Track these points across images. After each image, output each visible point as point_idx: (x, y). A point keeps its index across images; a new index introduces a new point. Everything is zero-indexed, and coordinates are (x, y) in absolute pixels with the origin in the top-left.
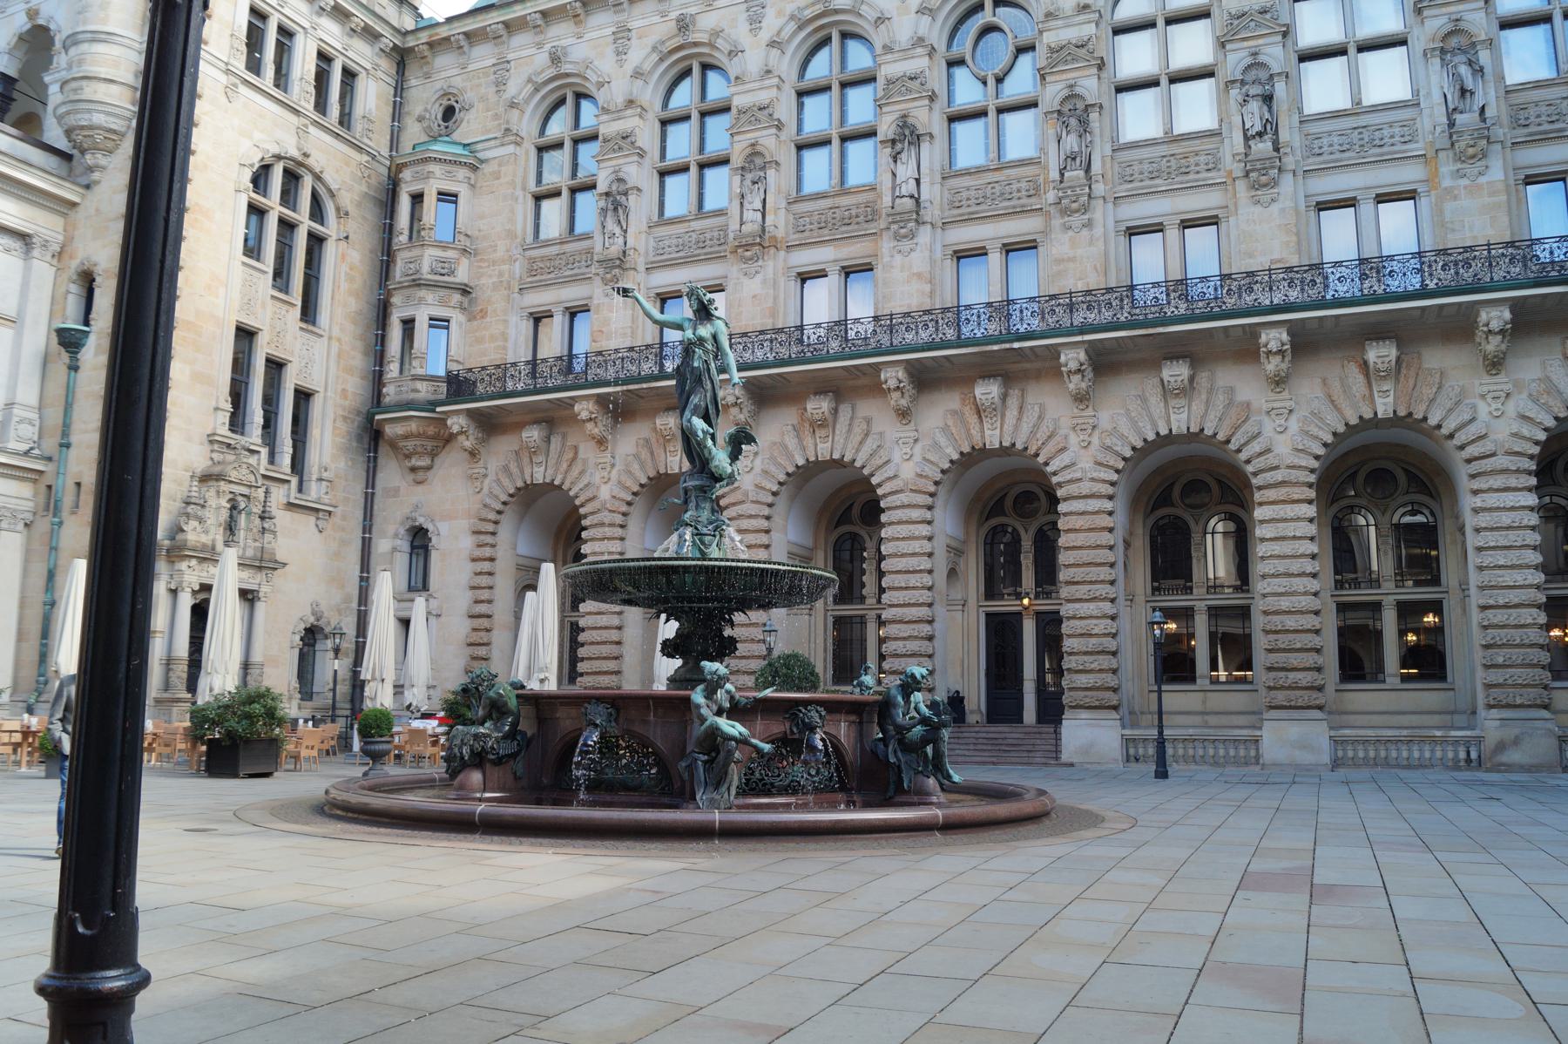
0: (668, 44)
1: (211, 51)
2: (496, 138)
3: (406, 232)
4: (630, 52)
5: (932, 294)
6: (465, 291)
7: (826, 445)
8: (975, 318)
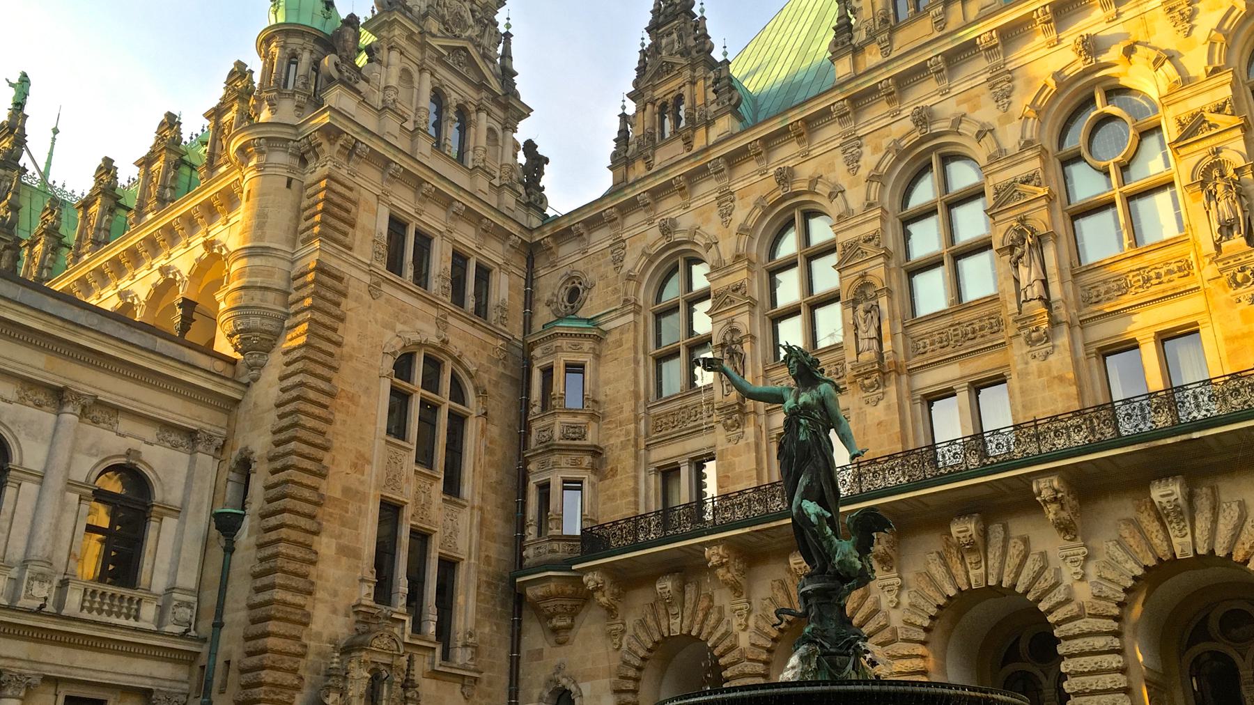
0: (768, 199)
1: (355, 255)
2: (616, 310)
3: (539, 404)
4: (734, 212)
5: (1081, 394)
6: (596, 452)
7: (978, 571)
8: (1138, 411)
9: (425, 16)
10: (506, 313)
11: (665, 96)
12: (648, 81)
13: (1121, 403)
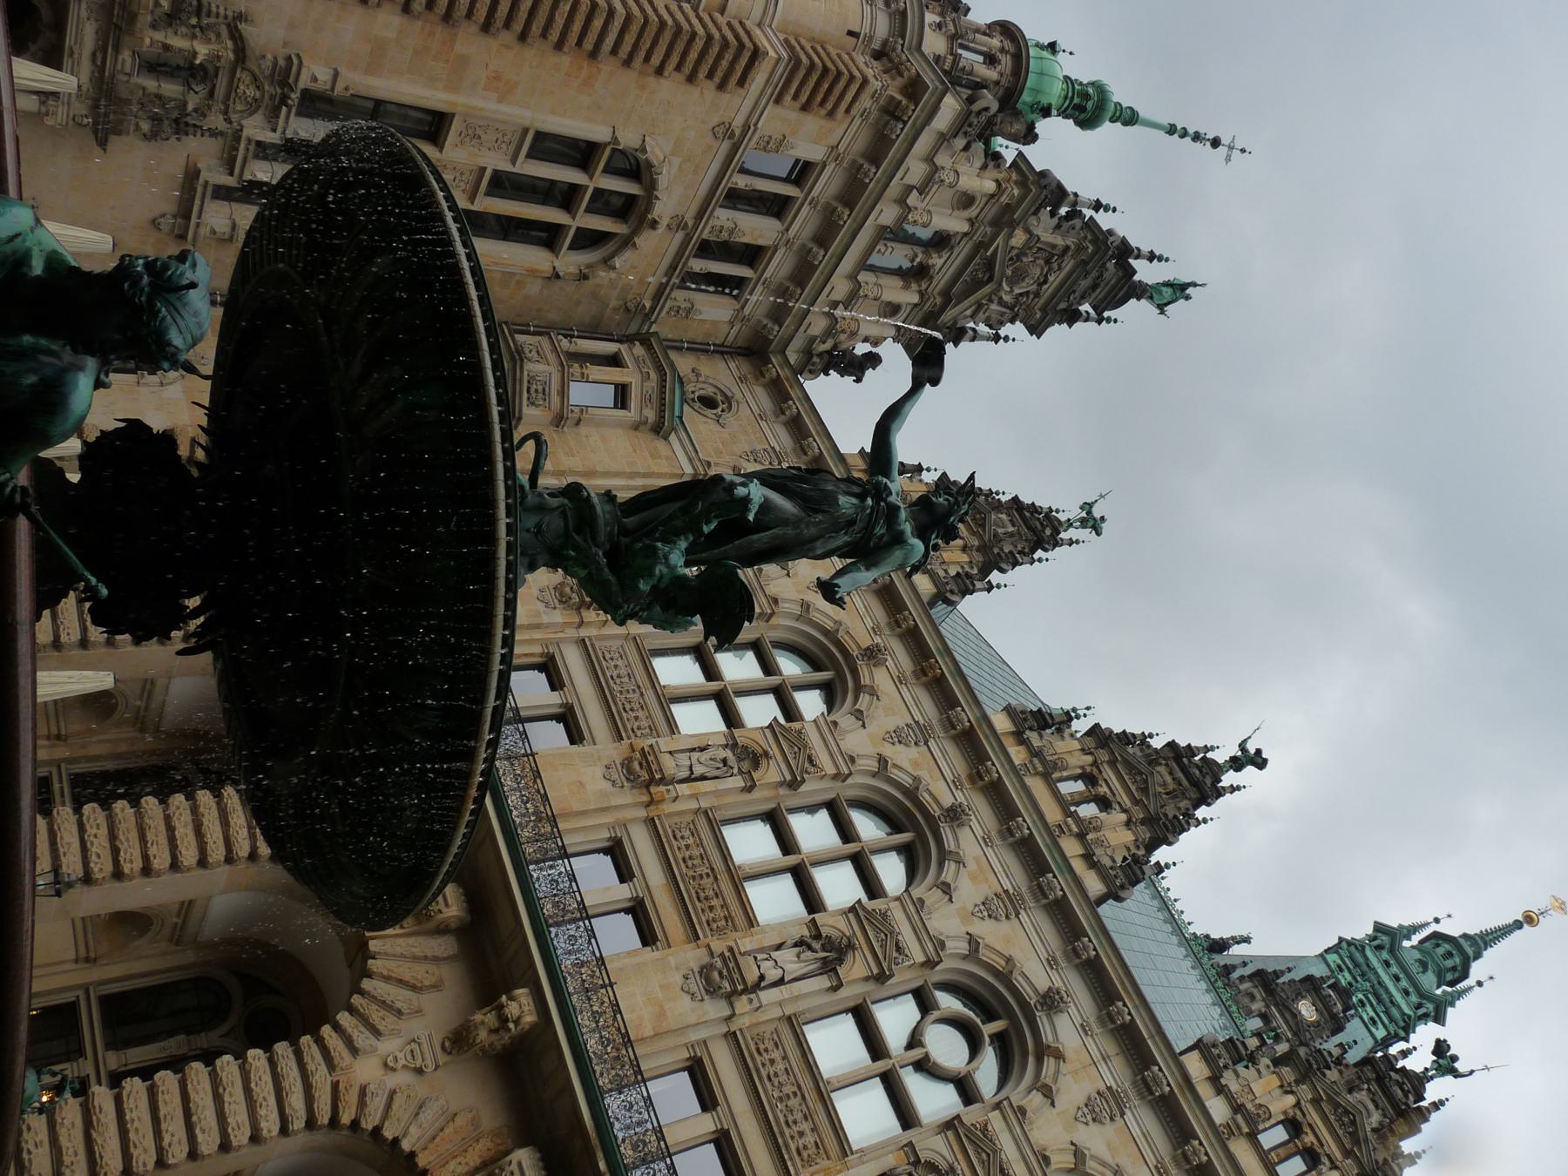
1: (769, 107)
3: (573, 348)
9: (1028, 231)
13: (645, 1094)
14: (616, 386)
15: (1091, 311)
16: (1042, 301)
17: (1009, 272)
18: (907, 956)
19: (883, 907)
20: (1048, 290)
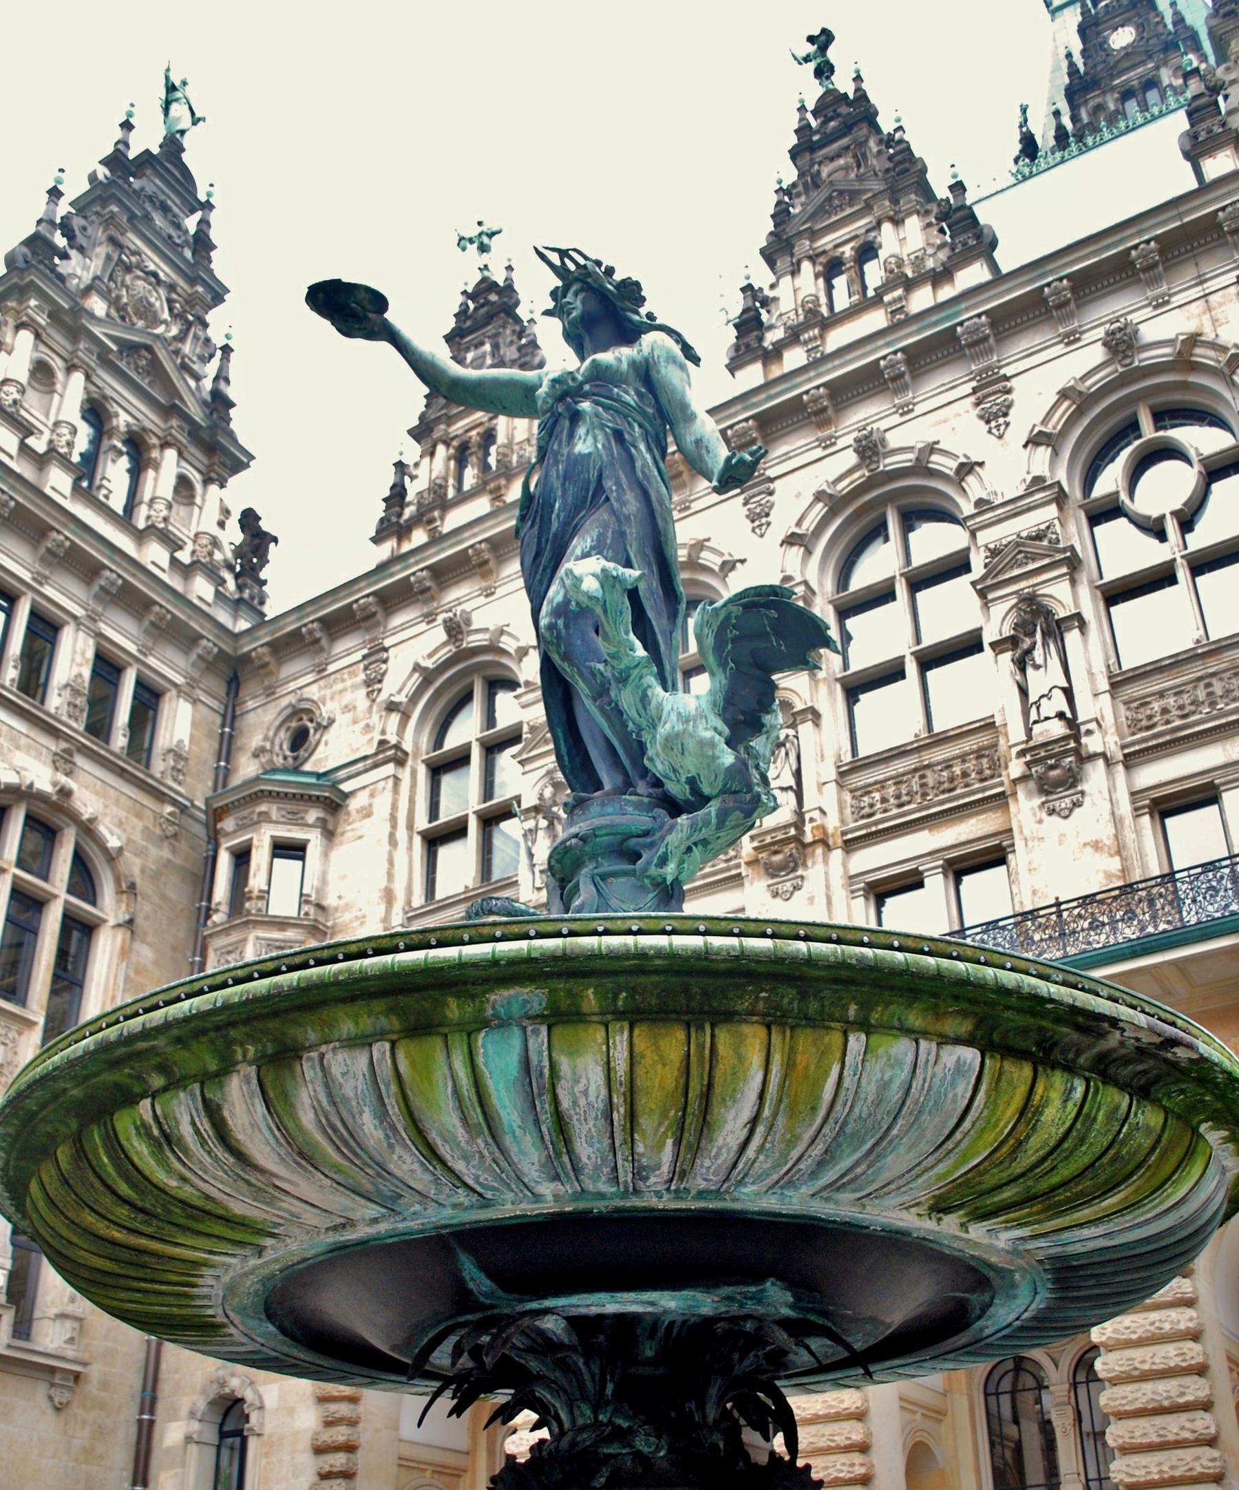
2: (365, 758)
10: (182, 763)
11: (467, 431)
12: (442, 409)
14: (275, 855)
15: (198, 215)
16: (181, 283)
17: (140, 324)
18: (1048, 528)
19: (983, 553)
20: (165, 272)
